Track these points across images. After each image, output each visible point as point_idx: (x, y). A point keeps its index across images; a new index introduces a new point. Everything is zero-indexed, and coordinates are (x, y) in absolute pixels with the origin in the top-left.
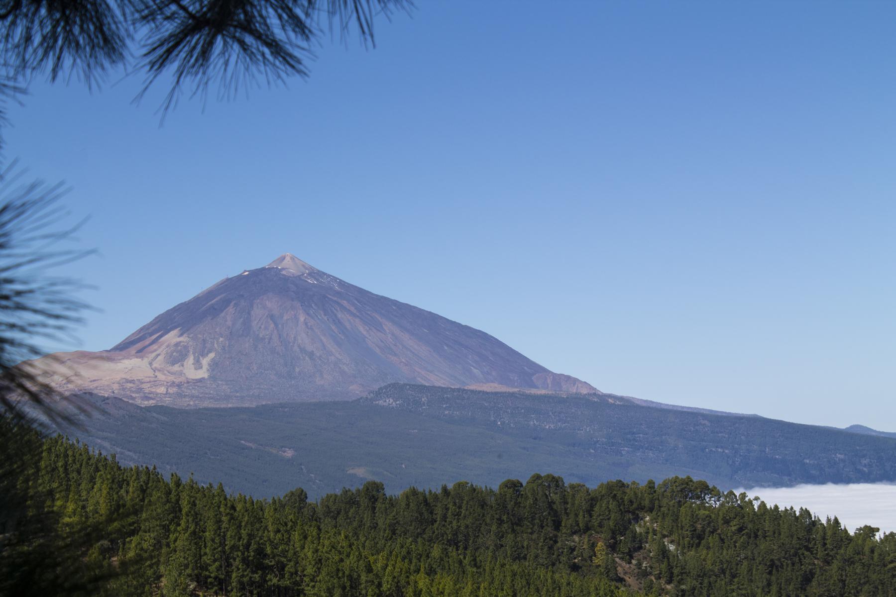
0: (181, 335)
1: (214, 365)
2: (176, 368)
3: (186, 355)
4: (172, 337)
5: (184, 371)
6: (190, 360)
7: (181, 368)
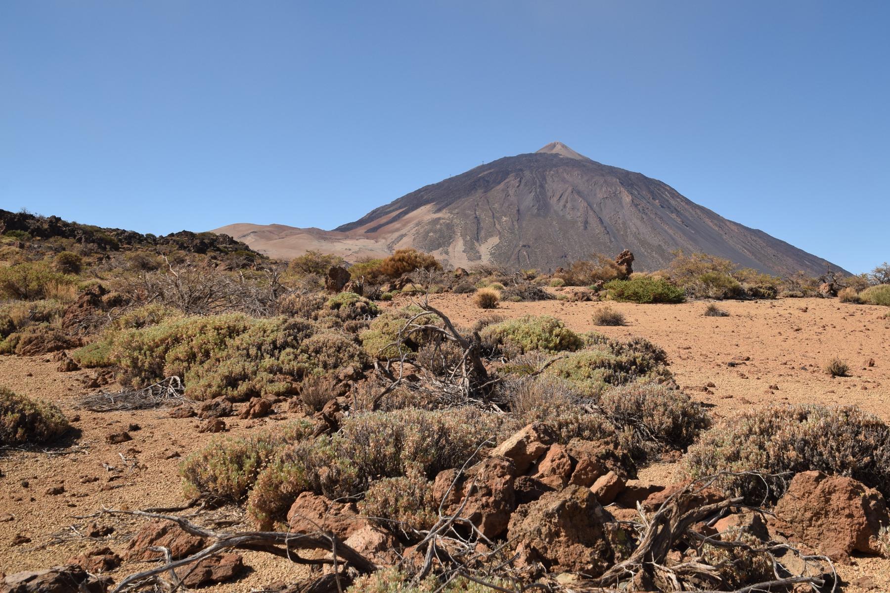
0: (439, 210)
3: (451, 237)
4: (424, 213)
6: (459, 246)
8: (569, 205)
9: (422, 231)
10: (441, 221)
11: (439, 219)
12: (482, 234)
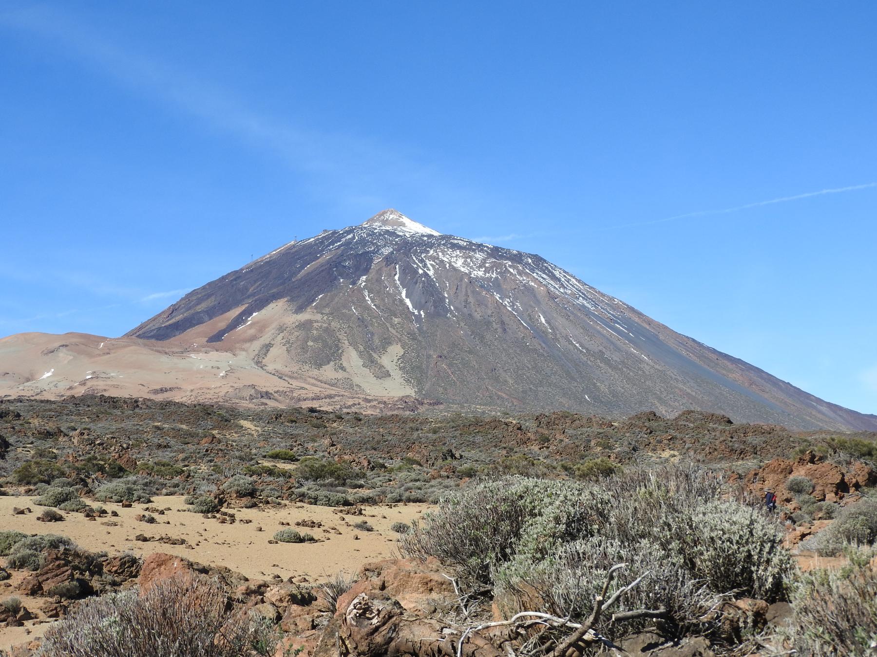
0: (300, 309)
1: (413, 370)
2: (329, 372)
4: (277, 312)
5: (356, 380)
7: (340, 375)
8: (471, 299)
9: (293, 338)
10: (315, 325)
11: (310, 322)
12: (377, 341)
